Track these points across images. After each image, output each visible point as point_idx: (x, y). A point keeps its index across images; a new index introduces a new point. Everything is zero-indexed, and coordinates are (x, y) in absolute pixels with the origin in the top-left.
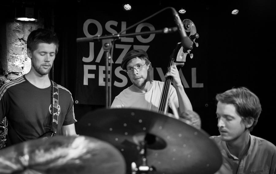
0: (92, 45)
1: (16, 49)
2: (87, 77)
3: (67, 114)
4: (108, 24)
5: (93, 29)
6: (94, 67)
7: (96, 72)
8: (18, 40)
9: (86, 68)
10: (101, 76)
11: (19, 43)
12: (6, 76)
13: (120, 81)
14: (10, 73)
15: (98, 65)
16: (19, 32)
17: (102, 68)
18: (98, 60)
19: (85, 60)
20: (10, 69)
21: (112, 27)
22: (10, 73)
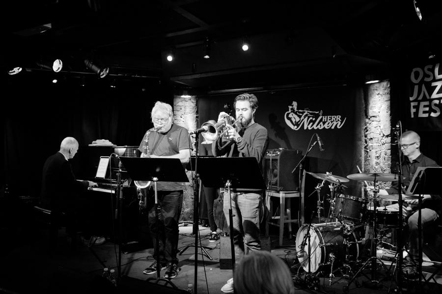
0: (416, 88)
1: (375, 101)
2: (413, 110)
3: (157, 142)
4: (426, 68)
5: (417, 75)
6: (416, 104)
7: (417, 107)
8: (377, 95)
9: (412, 104)
10: (422, 109)
11: (377, 96)
12: (369, 119)
13: (435, 112)
14: (371, 117)
15: (419, 102)
16: (376, 90)
17: (423, 104)
18: (420, 98)
19: (411, 99)
20: (371, 113)
21: (429, 70)
22: (371, 117)
